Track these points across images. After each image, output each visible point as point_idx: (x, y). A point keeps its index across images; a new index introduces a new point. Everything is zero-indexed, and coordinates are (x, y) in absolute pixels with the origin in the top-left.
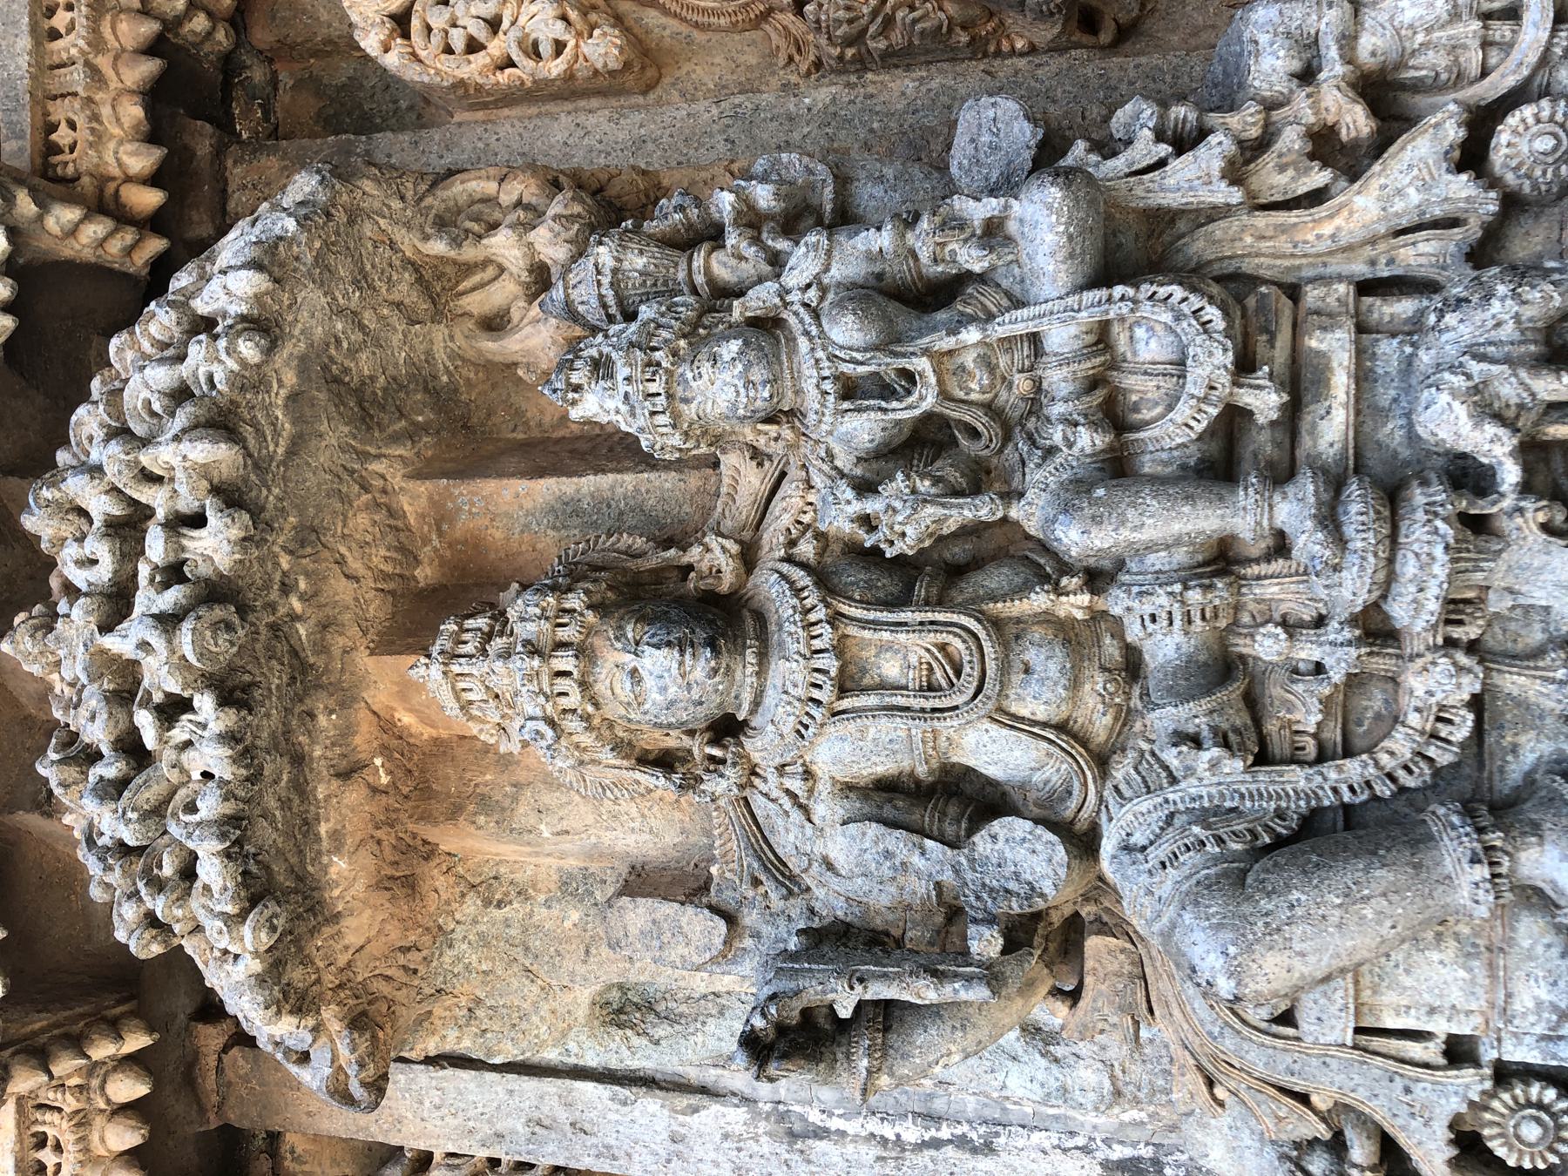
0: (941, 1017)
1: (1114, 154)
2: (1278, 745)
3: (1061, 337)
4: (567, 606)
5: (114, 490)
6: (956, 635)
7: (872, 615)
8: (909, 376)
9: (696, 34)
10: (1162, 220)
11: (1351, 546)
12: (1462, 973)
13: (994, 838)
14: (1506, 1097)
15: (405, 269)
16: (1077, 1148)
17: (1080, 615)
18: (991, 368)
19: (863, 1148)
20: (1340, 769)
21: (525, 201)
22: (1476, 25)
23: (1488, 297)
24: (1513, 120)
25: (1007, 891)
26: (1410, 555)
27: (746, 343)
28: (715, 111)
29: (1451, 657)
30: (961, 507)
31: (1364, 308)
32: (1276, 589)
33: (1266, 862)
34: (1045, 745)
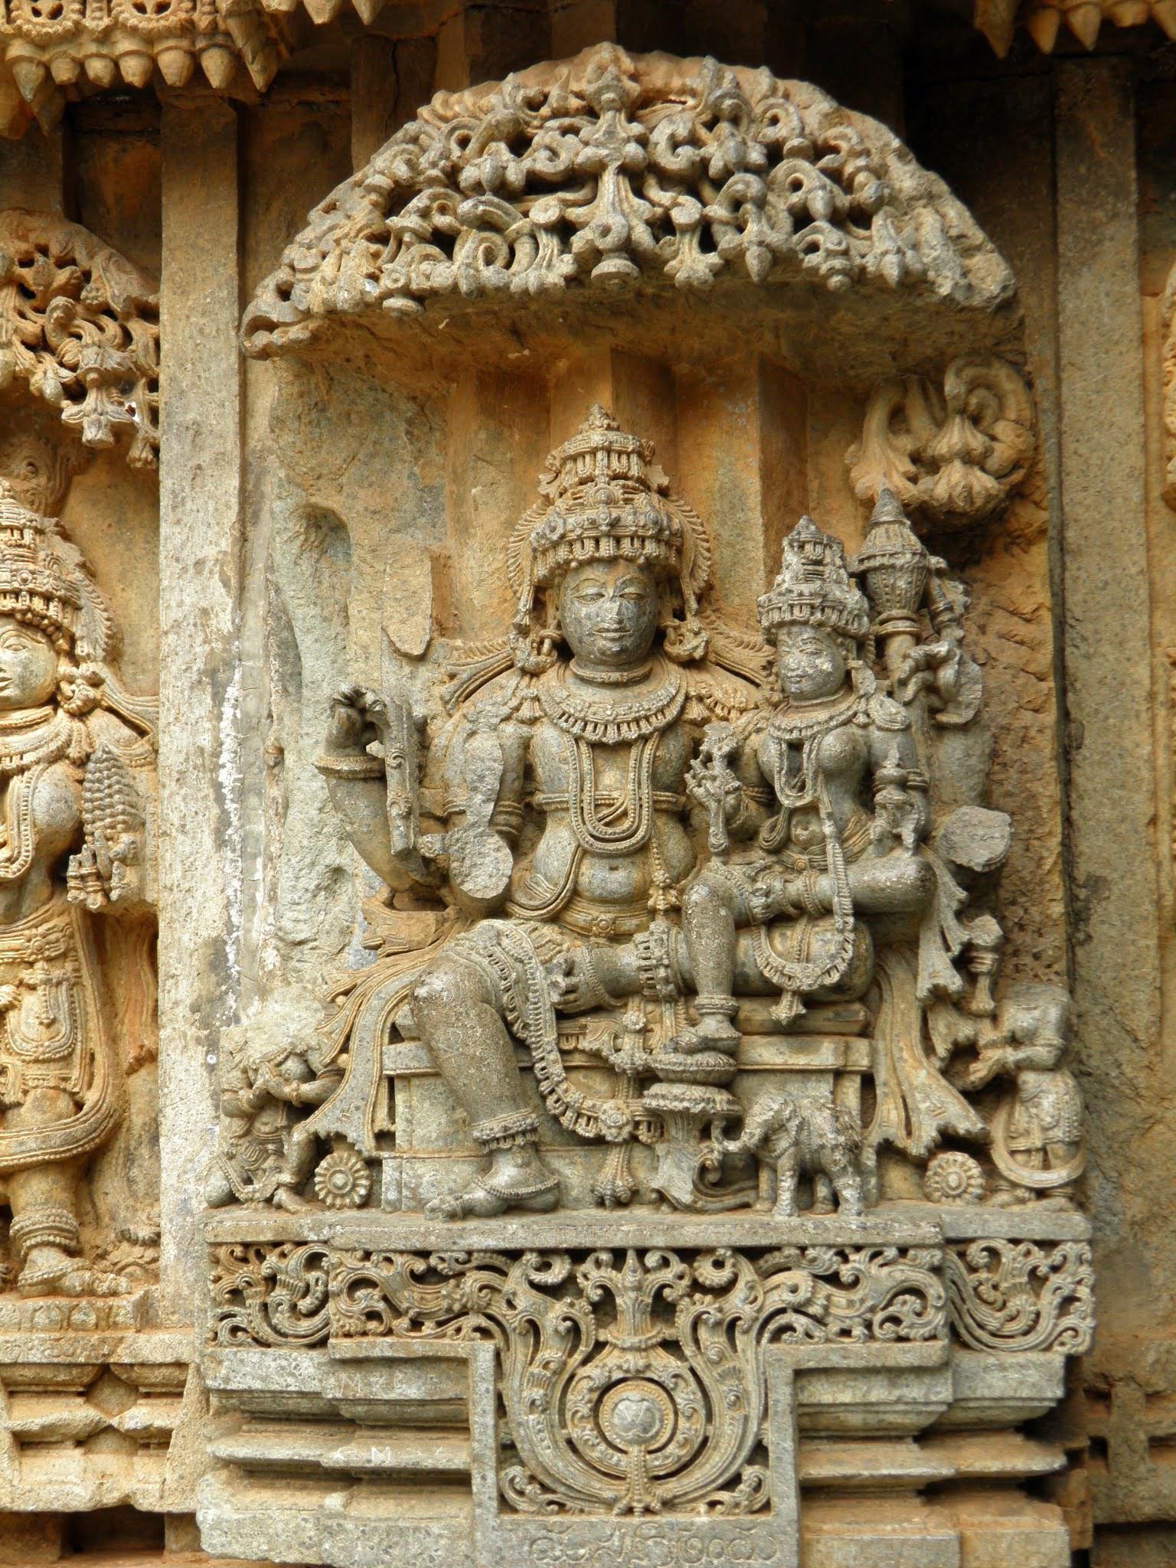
2: (569, 1027)
3: (824, 885)
4: (647, 543)
5: (728, 173)
7: (645, 765)
8: (802, 788)
12: (434, 1135)
13: (498, 850)
14: (358, 1166)
16: (230, 917)
17: (650, 903)
20: (555, 1062)
21: (996, 445)
22: (1039, 1144)
23: (838, 1132)
24: (971, 1162)
27: (829, 674)
31: (853, 1077)
33: (497, 1016)
34: (562, 882)
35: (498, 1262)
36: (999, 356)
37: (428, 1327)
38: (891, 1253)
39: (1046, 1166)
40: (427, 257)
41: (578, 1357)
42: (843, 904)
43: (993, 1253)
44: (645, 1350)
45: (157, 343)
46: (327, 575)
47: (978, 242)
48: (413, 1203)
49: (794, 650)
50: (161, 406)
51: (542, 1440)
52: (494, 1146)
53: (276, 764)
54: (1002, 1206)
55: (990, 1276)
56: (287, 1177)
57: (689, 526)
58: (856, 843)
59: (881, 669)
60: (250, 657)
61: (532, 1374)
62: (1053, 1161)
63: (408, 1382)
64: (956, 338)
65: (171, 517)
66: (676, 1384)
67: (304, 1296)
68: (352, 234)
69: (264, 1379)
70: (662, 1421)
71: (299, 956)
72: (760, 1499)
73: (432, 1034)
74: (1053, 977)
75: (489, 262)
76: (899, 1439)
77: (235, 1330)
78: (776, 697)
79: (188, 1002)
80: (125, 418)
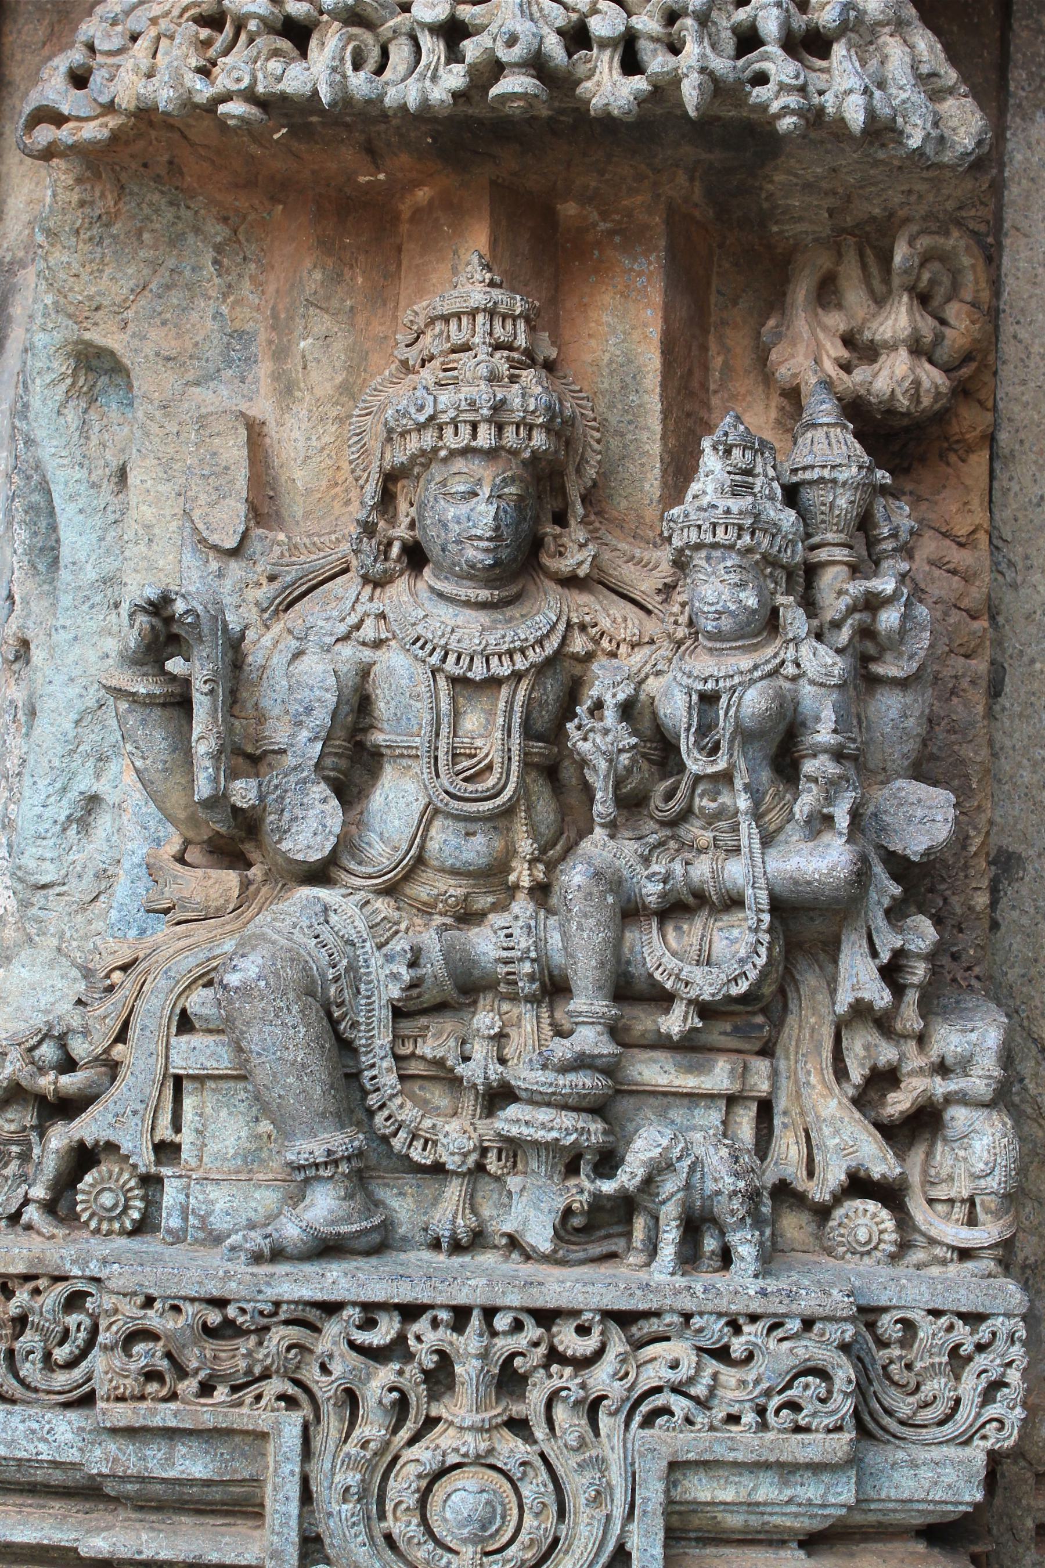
0: (174, 751)
2: (407, 1027)
4: (535, 433)
6: (499, 779)
7: (517, 708)
8: (715, 749)
11: (561, 1077)
12: (232, 1152)
13: (324, 801)
14: (132, 1183)
15: (885, 209)
17: (512, 878)
20: (389, 1070)
22: (965, 1194)
23: (736, 1175)
24: (885, 1214)
25: (283, 810)
26: (552, 1117)
27: (754, 612)
29: (474, 1150)
30: (606, 790)
31: (748, 1103)
32: (529, 1029)
33: (322, 1014)
34: (405, 846)
35: (313, 1315)
36: (959, 223)
37: (221, 1393)
38: (794, 1325)
39: (972, 1221)
40: (276, 53)
41: (404, 1434)
42: (758, 897)
43: (908, 1325)
44: (488, 1431)
46: (96, 429)
47: (950, 83)
48: (201, 1235)
49: (712, 579)
51: (356, 1536)
53: (17, 658)
54: (918, 1267)
55: (904, 1353)
56: (39, 1192)
57: (577, 410)
58: (773, 819)
59: (810, 605)
61: (348, 1455)
62: (981, 1215)
64: (913, 198)
66: (524, 1473)
67: (61, 1344)
68: (176, 12)
71: (43, 901)
73: (242, 1033)
74: (974, 982)
75: (357, 67)
76: (782, 1543)
78: (681, 632)
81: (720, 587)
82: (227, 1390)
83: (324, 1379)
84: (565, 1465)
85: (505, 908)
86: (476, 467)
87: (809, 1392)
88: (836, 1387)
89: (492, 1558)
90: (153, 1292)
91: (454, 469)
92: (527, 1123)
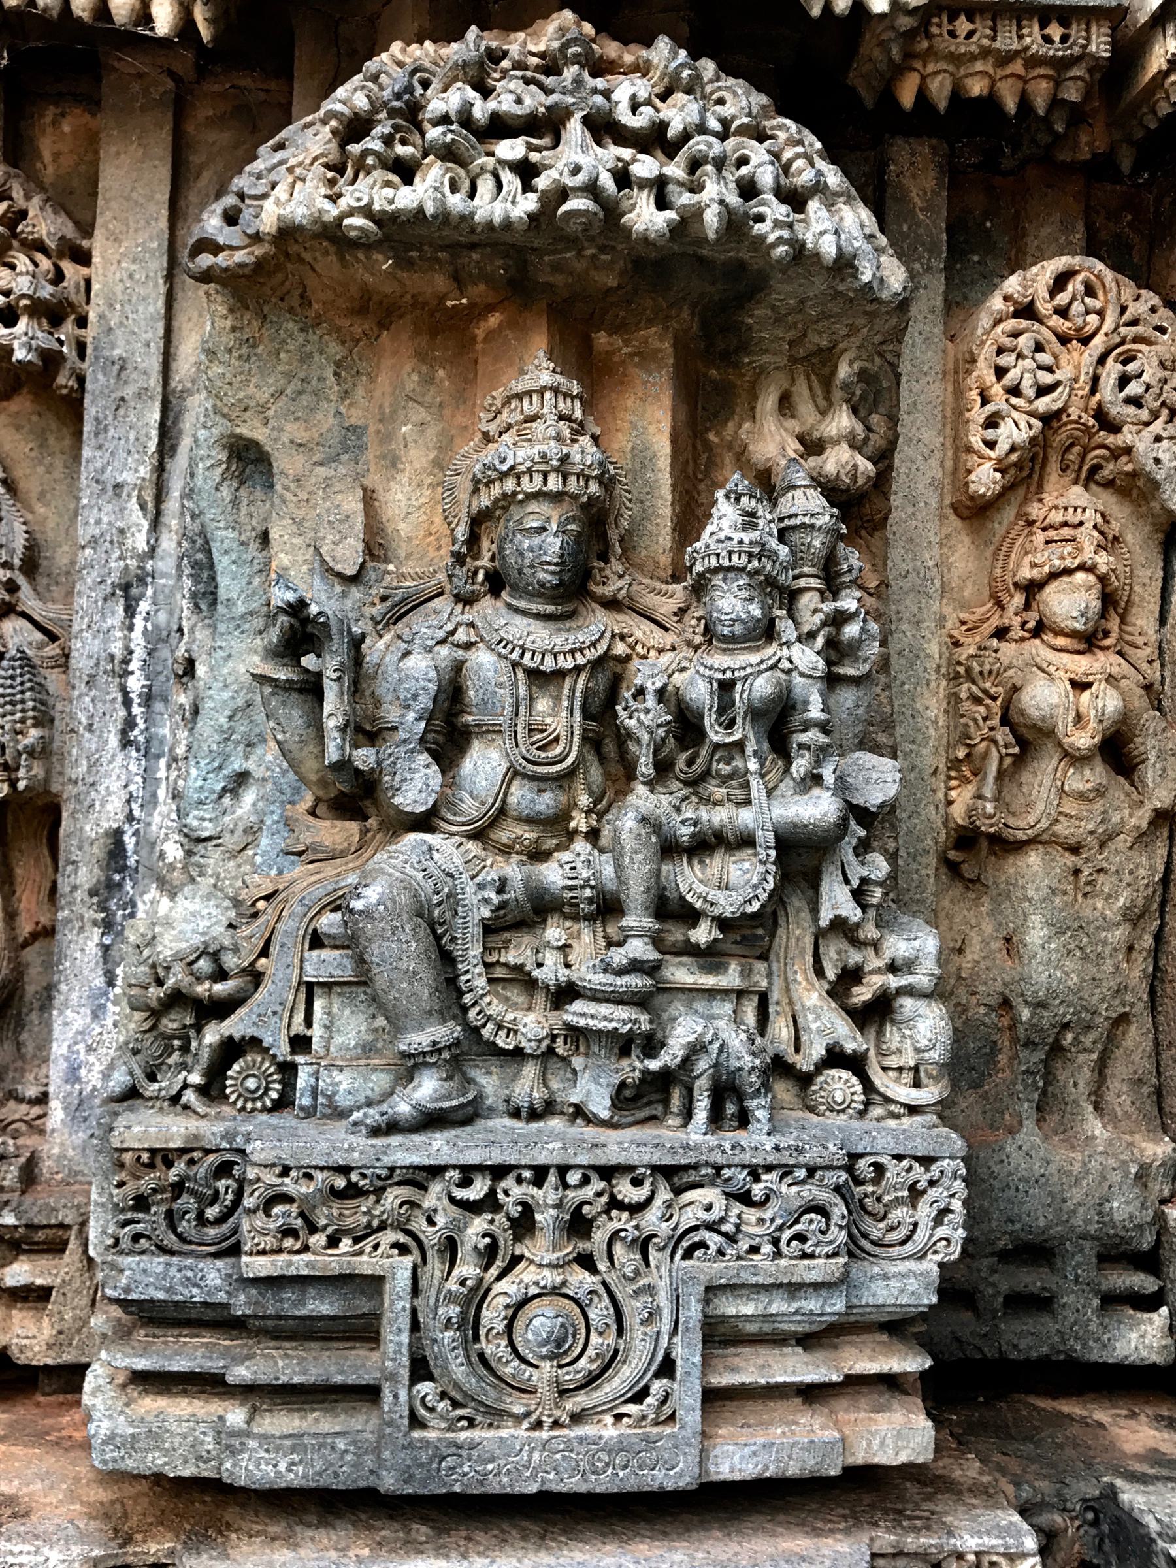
1: (857, 855)
2: (494, 941)
3: (746, 817)
4: (591, 483)
7: (578, 694)
8: (731, 724)
9: (992, 548)
10: (813, 882)
12: (353, 1043)
13: (427, 766)
14: (272, 1070)
17: (573, 824)
18: (731, 776)
19: (119, 644)
20: (480, 975)
22: (912, 1064)
23: (754, 1054)
24: (854, 1080)
27: (759, 620)
28: (931, 563)
34: (491, 801)
37: (346, 1245)
38: (801, 1174)
39: (917, 1084)
41: (494, 1271)
42: (765, 837)
45: (88, 282)
46: (245, 503)
48: (329, 1111)
50: (89, 340)
52: (420, 1060)
53: (185, 674)
54: (878, 1120)
56: (195, 1078)
60: (164, 575)
61: (450, 1291)
63: (322, 1298)
65: (93, 442)
68: (308, 162)
69: (168, 1290)
70: (574, 1336)
71: (203, 852)
72: (667, 1410)
77: (136, 1238)
79: (87, 887)
80: (56, 346)
81: (734, 601)
82: (350, 1242)
83: (430, 1229)
84: (623, 1292)
85: (567, 848)
86: (544, 508)
87: (813, 1227)
88: (833, 1222)
89: (565, 1370)
90: (290, 1162)
91: (529, 509)
92: (592, 1016)
